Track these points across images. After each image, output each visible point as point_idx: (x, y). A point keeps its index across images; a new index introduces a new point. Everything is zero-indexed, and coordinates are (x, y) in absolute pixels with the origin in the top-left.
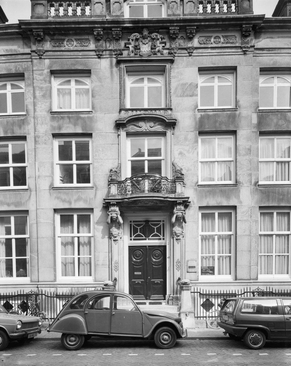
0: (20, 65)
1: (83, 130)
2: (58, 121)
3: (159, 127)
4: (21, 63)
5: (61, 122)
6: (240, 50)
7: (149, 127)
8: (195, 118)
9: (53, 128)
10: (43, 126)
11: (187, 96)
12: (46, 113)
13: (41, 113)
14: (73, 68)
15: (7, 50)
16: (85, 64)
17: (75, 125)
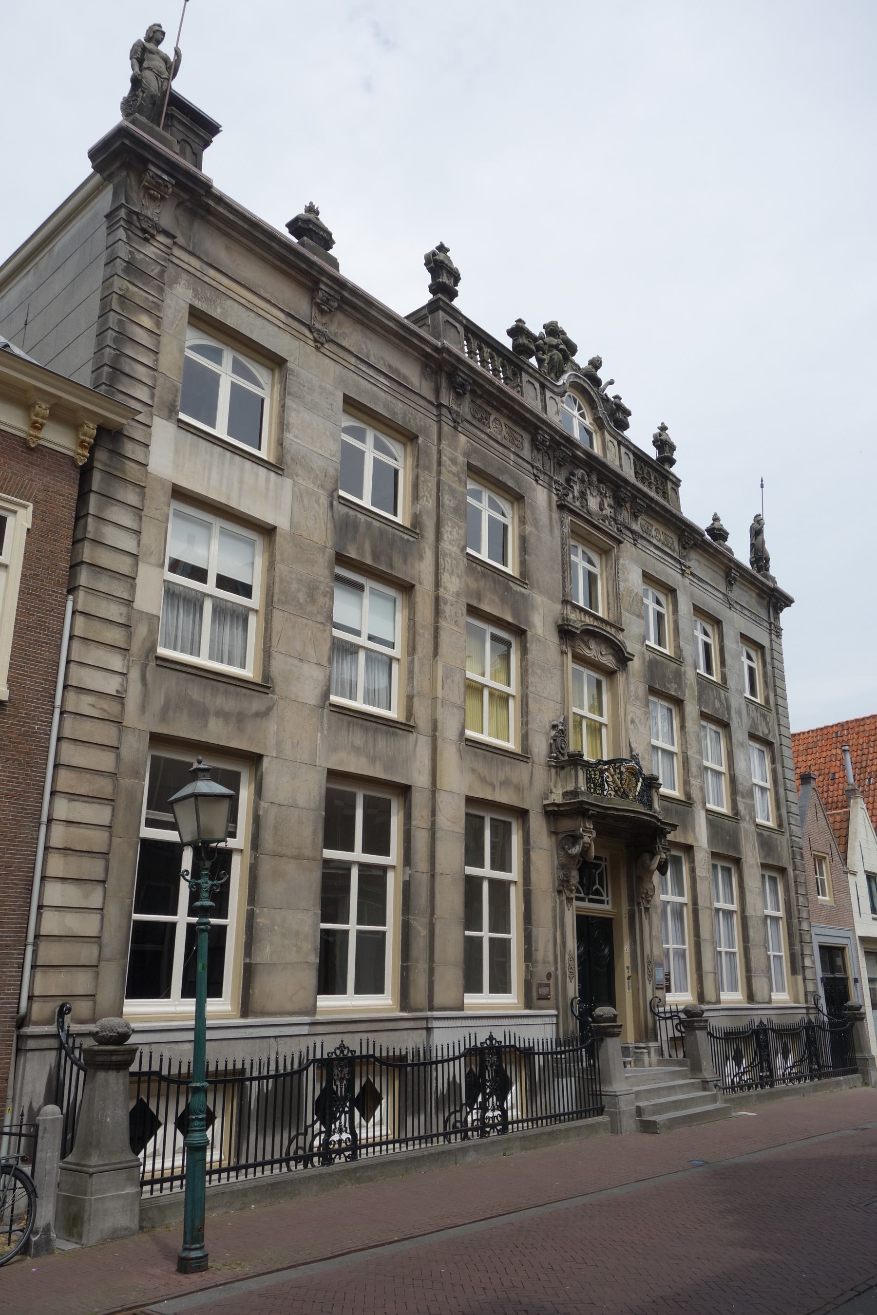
0: (411, 414)
1: (514, 618)
2: (477, 580)
3: (610, 657)
4: (414, 412)
5: (482, 583)
6: (678, 566)
7: (599, 655)
8: (644, 658)
9: (469, 593)
10: (453, 578)
11: (634, 614)
12: (458, 551)
13: (450, 547)
14: (500, 478)
15: (390, 366)
16: (517, 481)
17: (504, 601)
